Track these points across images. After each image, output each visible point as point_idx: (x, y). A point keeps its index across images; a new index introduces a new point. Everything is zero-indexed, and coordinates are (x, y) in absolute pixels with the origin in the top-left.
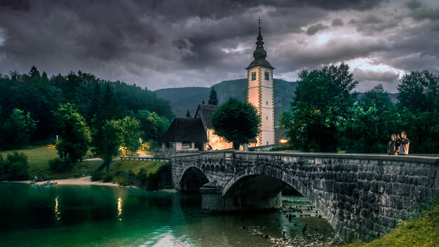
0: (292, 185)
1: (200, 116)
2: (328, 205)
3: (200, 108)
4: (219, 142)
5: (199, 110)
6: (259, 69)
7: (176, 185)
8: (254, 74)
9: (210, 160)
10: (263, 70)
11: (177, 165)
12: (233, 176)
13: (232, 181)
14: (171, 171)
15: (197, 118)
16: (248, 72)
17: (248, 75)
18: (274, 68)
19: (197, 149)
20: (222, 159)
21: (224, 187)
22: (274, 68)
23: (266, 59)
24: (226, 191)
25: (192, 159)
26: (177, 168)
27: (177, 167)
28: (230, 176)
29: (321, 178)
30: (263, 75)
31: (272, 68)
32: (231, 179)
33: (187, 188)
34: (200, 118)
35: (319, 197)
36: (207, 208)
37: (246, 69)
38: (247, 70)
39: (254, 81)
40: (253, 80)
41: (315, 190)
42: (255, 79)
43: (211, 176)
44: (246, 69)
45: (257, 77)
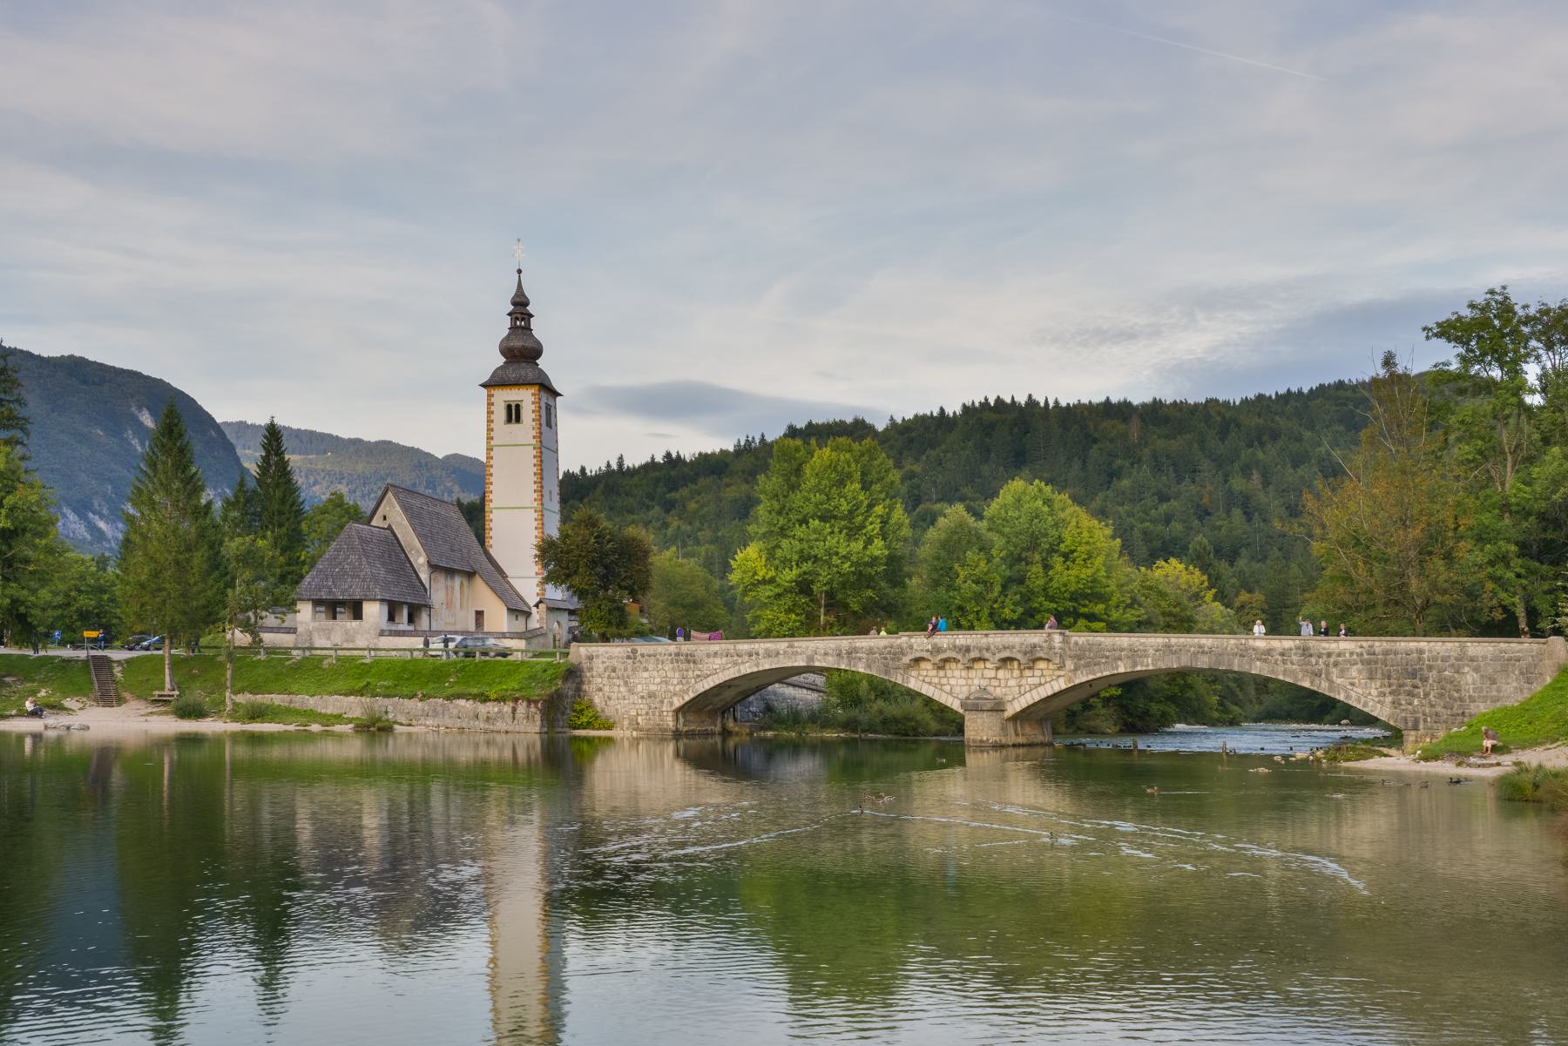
0: (1281, 678)
1: (388, 522)
2: (1370, 694)
3: (390, 495)
4: (444, 606)
5: (384, 501)
6: (533, 395)
7: (640, 718)
8: (513, 405)
9: (968, 649)
10: (545, 397)
11: (651, 667)
12: (1059, 676)
13: (1061, 685)
14: (582, 683)
15: (374, 523)
16: (490, 396)
17: (490, 404)
18: (561, 395)
19: (411, 628)
20: (1035, 646)
21: (1014, 699)
22: (561, 395)
23: (542, 363)
24: (1024, 705)
25: (790, 650)
26: (646, 674)
27: (646, 670)
28: (1042, 675)
29: (1354, 664)
30: (543, 412)
31: (556, 394)
32: (1046, 682)
33: (685, 725)
34: (390, 525)
35: (1349, 687)
36: (985, 738)
37: (484, 385)
38: (485, 391)
39: (514, 427)
40: (509, 420)
41: (1339, 681)
42: (518, 420)
43: (936, 680)
44: (484, 385)
45: (528, 413)
